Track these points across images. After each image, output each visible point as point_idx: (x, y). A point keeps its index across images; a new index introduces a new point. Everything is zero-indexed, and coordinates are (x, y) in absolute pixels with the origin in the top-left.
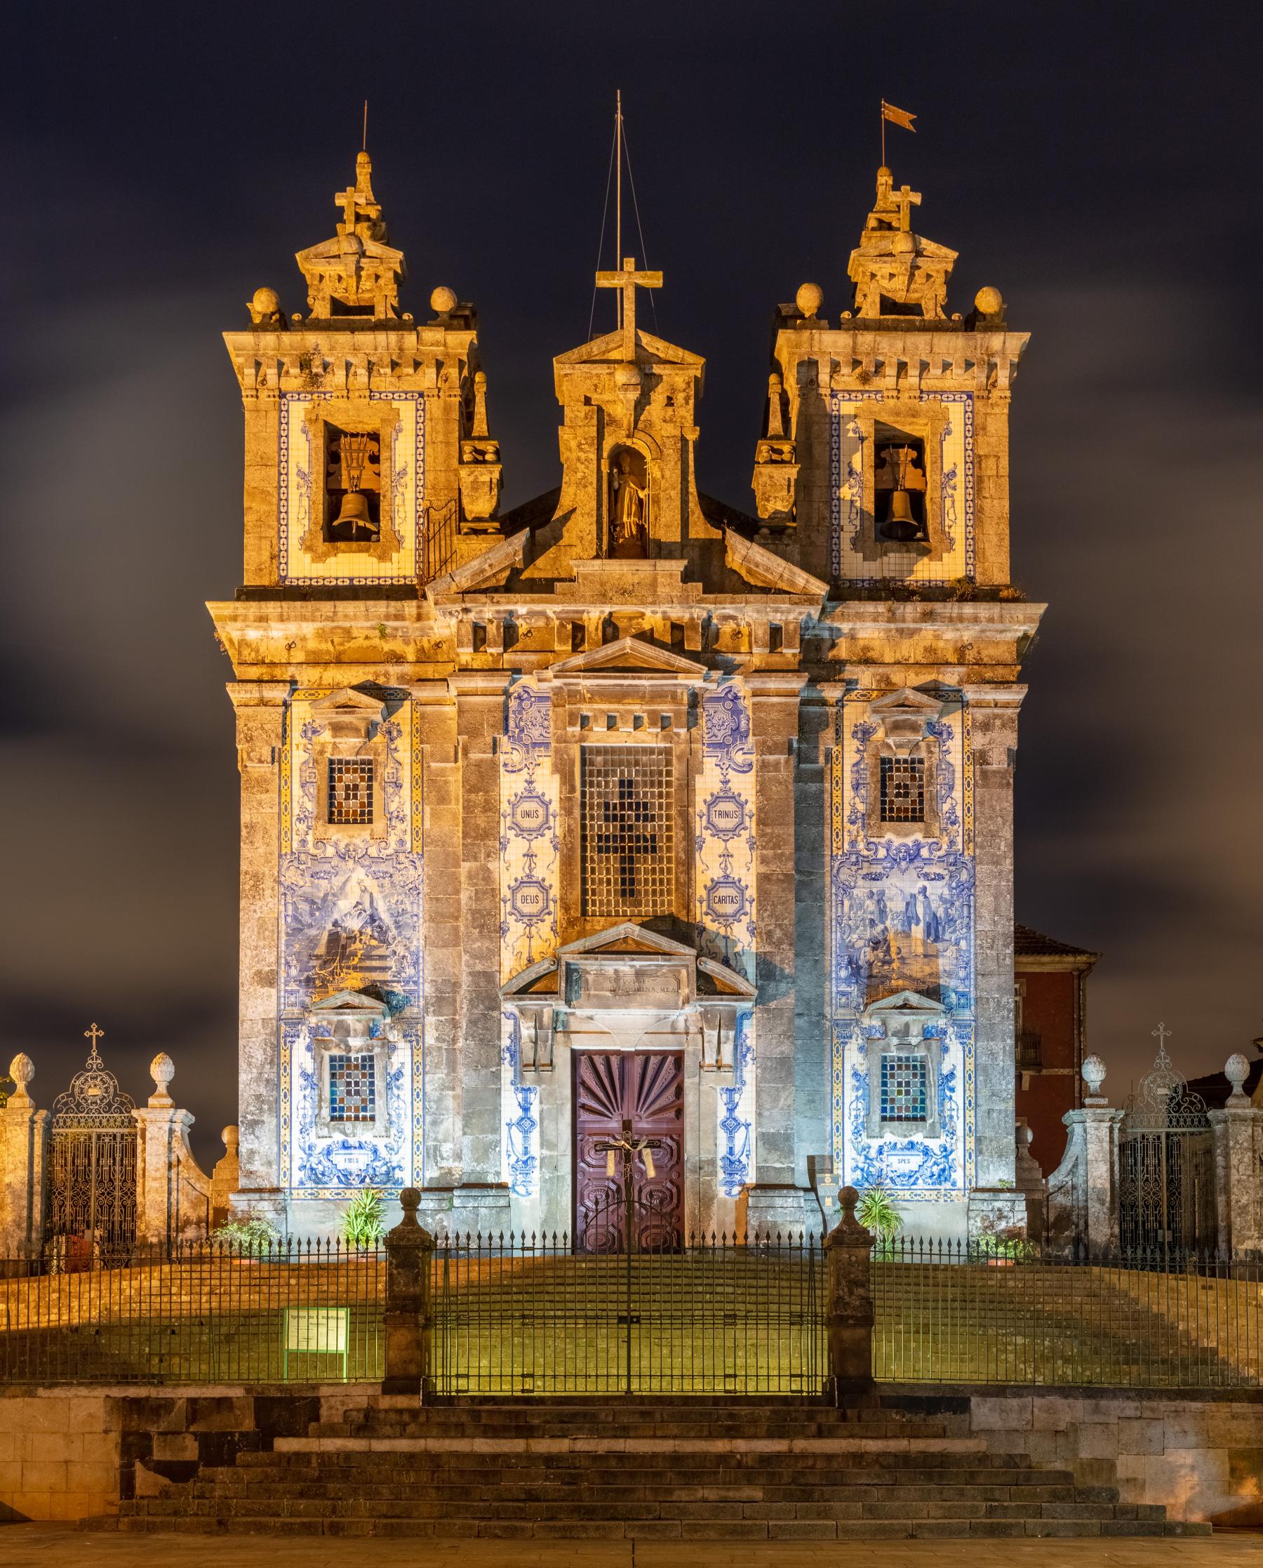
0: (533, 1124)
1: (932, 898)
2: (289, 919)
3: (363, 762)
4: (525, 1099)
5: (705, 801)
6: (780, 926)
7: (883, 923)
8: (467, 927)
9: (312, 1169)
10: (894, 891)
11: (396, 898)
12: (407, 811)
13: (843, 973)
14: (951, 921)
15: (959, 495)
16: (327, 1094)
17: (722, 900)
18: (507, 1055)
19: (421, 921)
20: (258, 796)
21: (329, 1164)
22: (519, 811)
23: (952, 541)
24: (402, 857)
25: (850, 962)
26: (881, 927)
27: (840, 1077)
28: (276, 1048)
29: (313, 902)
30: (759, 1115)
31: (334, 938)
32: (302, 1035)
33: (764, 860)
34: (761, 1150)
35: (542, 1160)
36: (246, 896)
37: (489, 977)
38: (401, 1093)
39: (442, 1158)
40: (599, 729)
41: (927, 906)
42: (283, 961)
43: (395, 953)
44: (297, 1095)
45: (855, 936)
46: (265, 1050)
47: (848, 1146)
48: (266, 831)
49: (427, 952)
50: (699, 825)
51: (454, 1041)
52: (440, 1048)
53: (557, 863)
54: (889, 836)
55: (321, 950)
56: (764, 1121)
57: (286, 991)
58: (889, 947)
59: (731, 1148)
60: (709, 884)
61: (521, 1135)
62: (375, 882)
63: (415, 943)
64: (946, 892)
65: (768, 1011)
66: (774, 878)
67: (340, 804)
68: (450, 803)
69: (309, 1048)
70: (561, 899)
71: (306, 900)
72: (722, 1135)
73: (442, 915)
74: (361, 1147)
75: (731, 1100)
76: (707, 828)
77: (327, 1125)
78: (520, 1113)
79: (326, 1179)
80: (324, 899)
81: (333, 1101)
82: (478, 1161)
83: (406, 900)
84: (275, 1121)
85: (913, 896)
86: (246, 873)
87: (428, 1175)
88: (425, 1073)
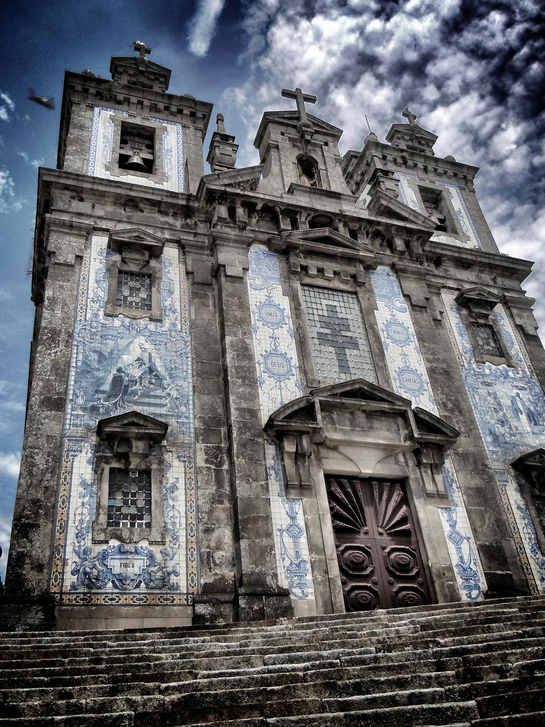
0: (301, 531)
1: (524, 399)
2: (79, 364)
3: (143, 276)
4: (291, 509)
5: (383, 323)
6: (450, 400)
7: (502, 410)
8: (232, 377)
9: (86, 573)
10: (502, 394)
11: (170, 358)
12: (179, 308)
13: (489, 439)
14: (539, 414)
15: (466, 220)
16: (105, 501)
17: (408, 380)
18: (272, 472)
19: (190, 376)
20: (61, 283)
21: (104, 569)
22: (263, 311)
23: (468, 237)
24: (173, 333)
25: (491, 433)
26: (501, 413)
27: (509, 508)
28: (58, 460)
29: (100, 354)
30: (475, 531)
31: (117, 381)
32: (84, 451)
33: (428, 360)
34: (483, 558)
35: (313, 564)
36: (44, 344)
37: (253, 413)
38: (175, 503)
39: (216, 565)
40: (313, 271)
41: (523, 404)
42: (71, 392)
43: (169, 395)
44: (75, 502)
45: (488, 417)
46: (47, 461)
47: (531, 561)
48: (65, 304)
49: (196, 397)
50: (383, 336)
51: (220, 464)
52: (209, 469)
53: (294, 345)
54: (487, 363)
55: (106, 387)
56: (480, 536)
57: (72, 415)
58: (510, 425)
59: (461, 557)
60: (397, 370)
61: (291, 540)
62: (153, 347)
63: (186, 389)
64: (531, 397)
65: (457, 454)
66: (438, 371)
67: (125, 298)
68: (209, 306)
69: (89, 462)
70: (300, 367)
71: (95, 351)
72: (452, 547)
73: (206, 373)
74: (136, 552)
75: (450, 519)
76: (388, 338)
77: (104, 531)
78: (289, 521)
79: (100, 584)
80: (111, 353)
81: (110, 507)
82: (255, 563)
83: (178, 360)
84: (50, 525)
85: (513, 397)
86: (46, 328)
87: (202, 581)
88: (198, 488)
